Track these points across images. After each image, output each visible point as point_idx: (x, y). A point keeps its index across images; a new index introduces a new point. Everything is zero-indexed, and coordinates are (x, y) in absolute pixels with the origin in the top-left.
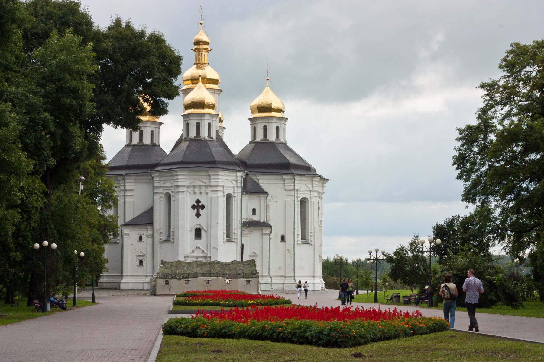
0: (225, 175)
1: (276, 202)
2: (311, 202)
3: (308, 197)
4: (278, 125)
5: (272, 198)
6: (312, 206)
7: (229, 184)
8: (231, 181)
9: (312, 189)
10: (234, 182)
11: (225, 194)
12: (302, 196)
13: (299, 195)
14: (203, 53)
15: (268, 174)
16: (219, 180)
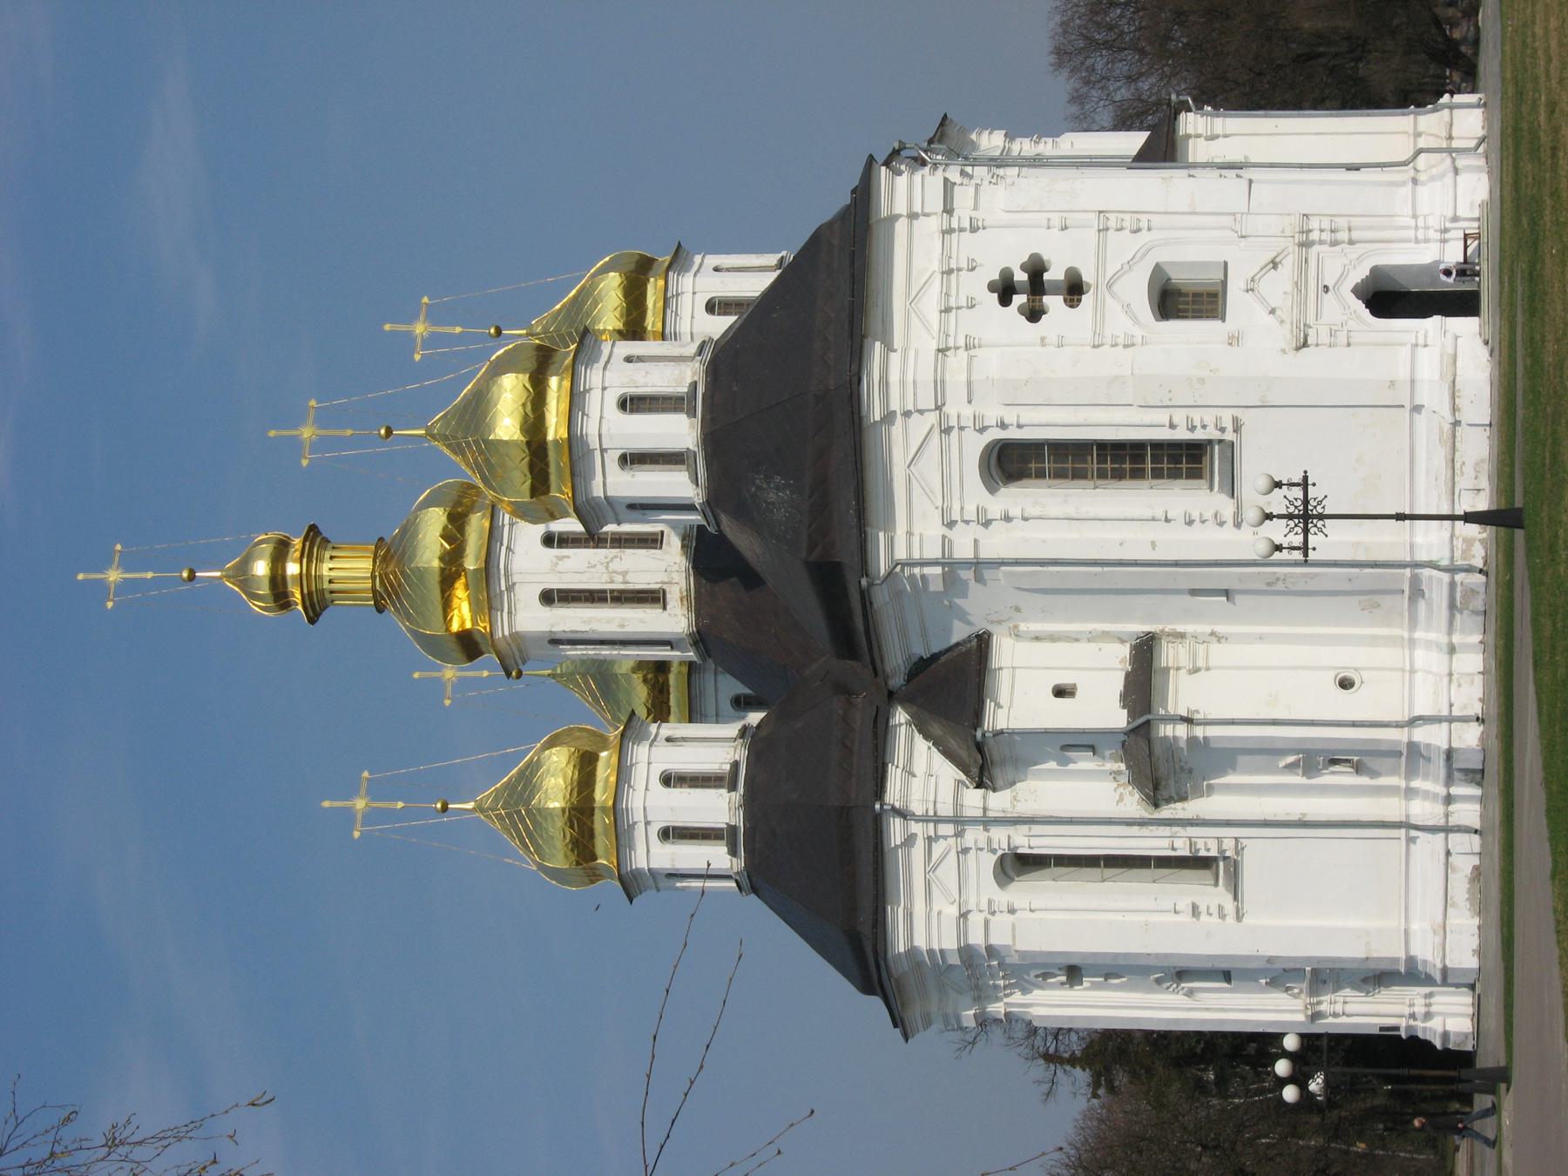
0: (909, 916)
1: (1018, 609)
2: (1003, 425)
3: (976, 445)
4: (612, 458)
5: (999, 622)
6: (1028, 416)
7: (948, 872)
8: (931, 866)
9: (932, 418)
10: (938, 848)
11: (1003, 897)
12: (974, 494)
13: (970, 514)
14: (327, 595)
15: (873, 637)
16: (936, 947)
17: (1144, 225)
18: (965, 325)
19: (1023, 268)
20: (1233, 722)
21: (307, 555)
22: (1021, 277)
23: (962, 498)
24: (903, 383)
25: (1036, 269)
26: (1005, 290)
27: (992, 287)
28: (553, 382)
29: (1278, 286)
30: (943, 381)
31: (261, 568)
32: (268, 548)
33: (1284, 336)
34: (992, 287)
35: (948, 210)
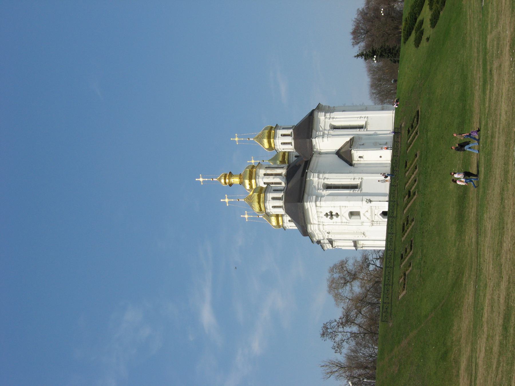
17: (347, 207)
18: (321, 220)
19: (329, 213)
20: (368, 247)
21: (229, 179)
22: (329, 214)
23: (325, 234)
24: (314, 229)
25: (331, 213)
26: (327, 215)
27: (325, 215)
28: (261, 203)
29: (368, 215)
30: (320, 229)
31: (223, 181)
32: (223, 178)
33: (370, 224)
34: (325, 215)
35: (316, 206)
